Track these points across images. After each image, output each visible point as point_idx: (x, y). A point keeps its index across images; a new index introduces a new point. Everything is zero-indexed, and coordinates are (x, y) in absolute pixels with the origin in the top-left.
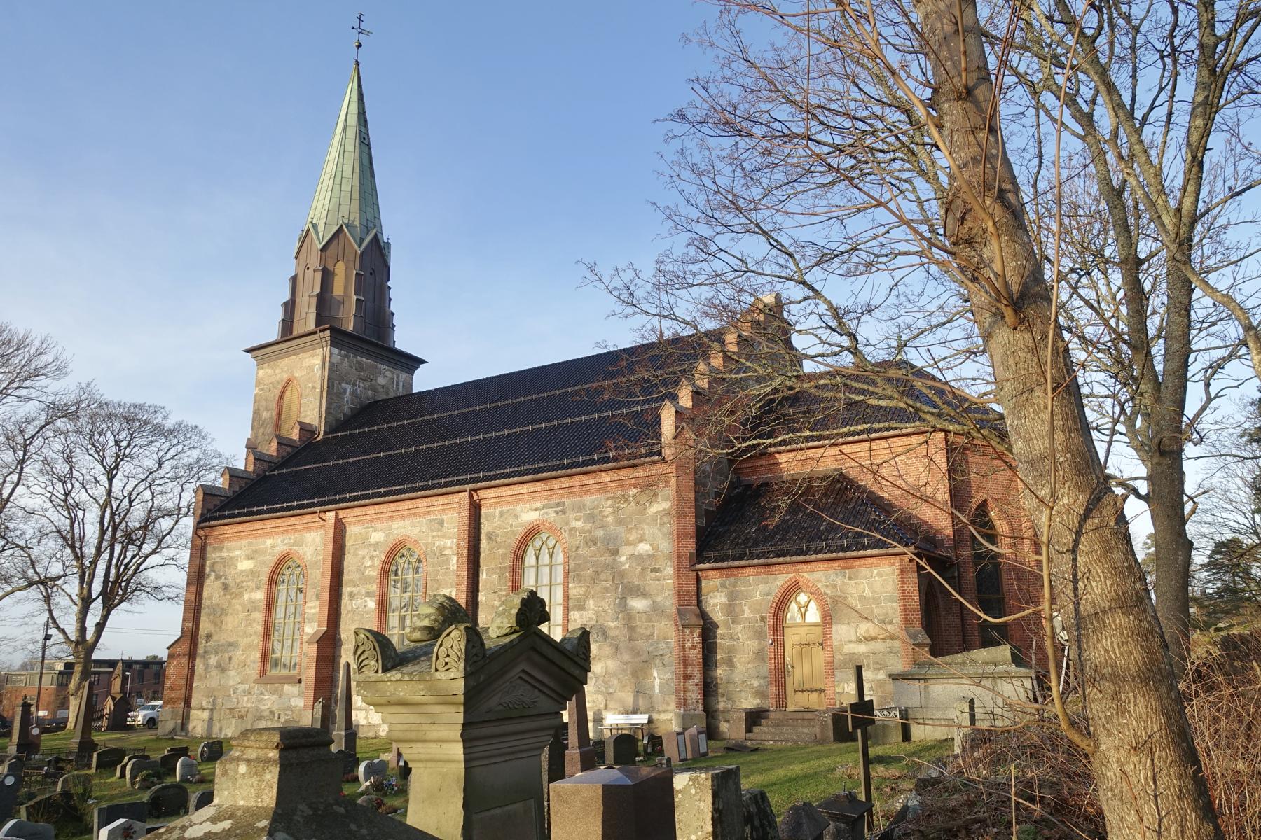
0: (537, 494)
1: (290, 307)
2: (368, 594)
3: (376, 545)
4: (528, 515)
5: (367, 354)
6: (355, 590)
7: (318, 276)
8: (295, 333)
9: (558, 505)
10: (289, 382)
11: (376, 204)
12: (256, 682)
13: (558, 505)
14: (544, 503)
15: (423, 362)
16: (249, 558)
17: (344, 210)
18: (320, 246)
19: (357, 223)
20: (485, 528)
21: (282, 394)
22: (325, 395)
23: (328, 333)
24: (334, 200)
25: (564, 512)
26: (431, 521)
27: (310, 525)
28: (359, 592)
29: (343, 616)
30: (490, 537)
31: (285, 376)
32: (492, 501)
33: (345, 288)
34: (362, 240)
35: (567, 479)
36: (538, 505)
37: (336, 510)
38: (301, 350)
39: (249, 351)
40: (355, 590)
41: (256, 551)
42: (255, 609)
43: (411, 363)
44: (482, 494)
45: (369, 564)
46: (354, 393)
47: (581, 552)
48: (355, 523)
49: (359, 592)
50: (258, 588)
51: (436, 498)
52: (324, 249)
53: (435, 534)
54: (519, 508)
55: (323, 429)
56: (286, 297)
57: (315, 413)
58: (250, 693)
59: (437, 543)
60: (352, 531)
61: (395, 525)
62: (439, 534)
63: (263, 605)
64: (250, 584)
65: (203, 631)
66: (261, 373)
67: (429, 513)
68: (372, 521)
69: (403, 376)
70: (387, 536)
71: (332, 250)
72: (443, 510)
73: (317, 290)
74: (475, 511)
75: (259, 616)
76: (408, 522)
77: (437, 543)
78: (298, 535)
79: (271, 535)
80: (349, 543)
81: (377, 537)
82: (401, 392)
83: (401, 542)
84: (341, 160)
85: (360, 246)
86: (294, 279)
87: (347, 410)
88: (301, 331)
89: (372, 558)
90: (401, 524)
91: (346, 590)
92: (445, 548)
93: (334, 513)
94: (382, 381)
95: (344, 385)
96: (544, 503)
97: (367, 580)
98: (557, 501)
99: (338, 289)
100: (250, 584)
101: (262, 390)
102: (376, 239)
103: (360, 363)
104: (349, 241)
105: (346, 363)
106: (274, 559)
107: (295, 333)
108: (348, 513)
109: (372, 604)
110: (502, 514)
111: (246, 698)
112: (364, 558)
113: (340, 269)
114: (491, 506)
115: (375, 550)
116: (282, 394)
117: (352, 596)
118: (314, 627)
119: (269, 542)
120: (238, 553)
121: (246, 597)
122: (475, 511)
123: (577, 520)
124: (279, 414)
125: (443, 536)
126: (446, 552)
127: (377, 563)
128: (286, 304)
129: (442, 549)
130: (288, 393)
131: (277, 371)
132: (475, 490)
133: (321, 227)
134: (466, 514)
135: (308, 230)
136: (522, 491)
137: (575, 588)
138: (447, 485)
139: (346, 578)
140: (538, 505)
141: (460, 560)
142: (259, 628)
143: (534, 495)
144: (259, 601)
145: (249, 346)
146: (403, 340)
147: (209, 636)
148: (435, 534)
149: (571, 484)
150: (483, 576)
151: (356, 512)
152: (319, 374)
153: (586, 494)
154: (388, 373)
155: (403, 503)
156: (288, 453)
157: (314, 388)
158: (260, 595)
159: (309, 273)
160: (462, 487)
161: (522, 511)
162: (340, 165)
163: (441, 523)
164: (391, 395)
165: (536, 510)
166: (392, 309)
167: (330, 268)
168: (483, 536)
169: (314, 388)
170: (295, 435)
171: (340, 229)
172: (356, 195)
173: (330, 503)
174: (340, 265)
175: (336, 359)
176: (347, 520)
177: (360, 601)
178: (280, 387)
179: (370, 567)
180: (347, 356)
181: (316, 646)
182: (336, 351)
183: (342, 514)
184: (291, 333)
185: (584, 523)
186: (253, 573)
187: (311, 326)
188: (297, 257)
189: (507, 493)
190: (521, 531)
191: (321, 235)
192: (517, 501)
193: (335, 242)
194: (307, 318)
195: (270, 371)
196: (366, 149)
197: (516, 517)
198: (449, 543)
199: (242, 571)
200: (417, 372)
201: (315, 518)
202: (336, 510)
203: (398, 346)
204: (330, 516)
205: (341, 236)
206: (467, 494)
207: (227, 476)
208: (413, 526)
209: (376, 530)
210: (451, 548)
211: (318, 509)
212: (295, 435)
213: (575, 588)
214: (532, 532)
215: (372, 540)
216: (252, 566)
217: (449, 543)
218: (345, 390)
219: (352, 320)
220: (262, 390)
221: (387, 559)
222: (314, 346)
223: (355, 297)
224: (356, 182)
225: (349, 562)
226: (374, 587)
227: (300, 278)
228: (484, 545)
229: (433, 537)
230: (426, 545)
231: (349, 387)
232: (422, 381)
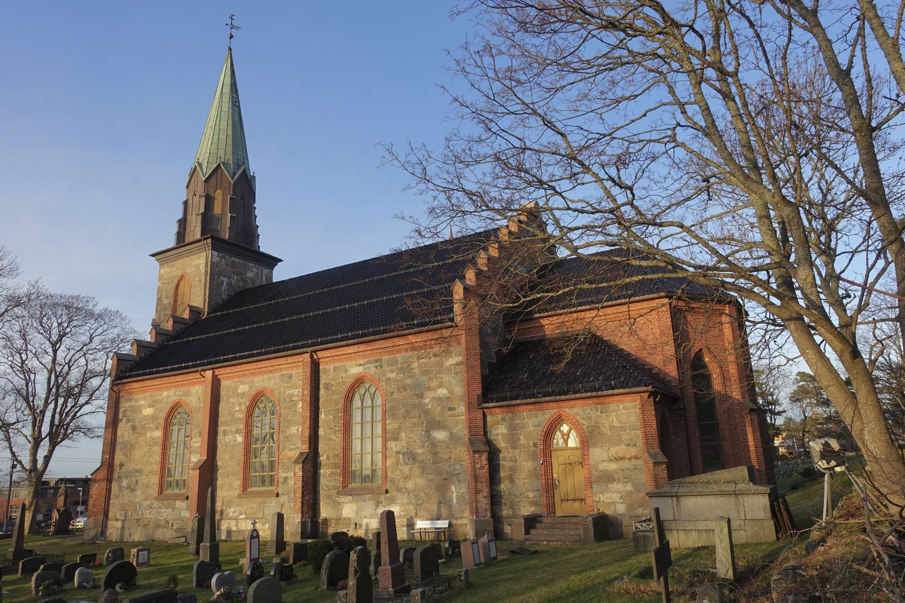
0: (361, 354)
1: (183, 223)
2: (237, 432)
3: (243, 394)
4: (355, 370)
5: (239, 256)
6: (227, 428)
7: (203, 200)
8: (187, 241)
9: (377, 361)
10: (182, 277)
11: (244, 149)
12: (155, 499)
13: (377, 361)
14: (366, 360)
15: (280, 261)
16: (150, 406)
17: (221, 153)
18: (204, 179)
19: (231, 162)
20: (323, 380)
21: (178, 286)
22: (208, 285)
23: (209, 240)
24: (214, 146)
25: (381, 366)
26: (282, 375)
27: (194, 381)
28: (230, 431)
29: (219, 449)
30: (327, 387)
31: (179, 273)
32: (328, 359)
33: (223, 209)
34: (234, 174)
35: (383, 341)
36: (362, 361)
37: (213, 369)
38: (191, 253)
39: (153, 255)
40: (227, 428)
41: (155, 401)
42: (155, 444)
43: (272, 261)
44: (320, 354)
45: (238, 409)
46: (229, 284)
47: (395, 396)
48: (227, 379)
49: (230, 431)
50: (157, 428)
51: (286, 358)
52: (206, 181)
53: (285, 385)
54: (347, 364)
55: (206, 310)
56: (180, 216)
57: (201, 298)
58: (151, 508)
60: (225, 384)
61: (257, 379)
62: (289, 385)
63: (160, 441)
64: (151, 425)
65: (117, 461)
66: (163, 271)
67: (281, 369)
68: (239, 376)
69: (265, 271)
70: (250, 388)
71: (213, 181)
72: (291, 367)
73: (202, 210)
74: (315, 367)
75: (158, 450)
76: (266, 376)
77: (287, 392)
78: (186, 388)
79: (167, 389)
80: (223, 393)
81: (243, 388)
82: (264, 282)
83: (261, 392)
84: (219, 117)
85: (233, 178)
86: (186, 203)
87: (224, 296)
88: (191, 240)
89: (240, 404)
90: (261, 378)
91: (221, 429)
92: (293, 395)
93: (211, 371)
94: (250, 275)
95: (222, 278)
96: (366, 360)
97: (237, 420)
98: (376, 358)
99: (217, 209)
100: (151, 425)
101: (163, 283)
102: (245, 173)
103: (233, 262)
104: (225, 175)
105: (224, 262)
106: (169, 406)
107: (187, 241)
108: (222, 371)
109: (240, 439)
110: (335, 369)
111: (148, 511)
112: (234, 404)
113: (218, 195)
114: (327, 363)
115: (242, 398)
116: (178, 286)
117: (225, 433)
118: (197, 457)
119: (165, 394)
120: (142, 402)
121: (148, 435)
122: (315, 367)
123: (391, 372)
124: (175, 301)
125: (292, 387)
126: (294, 399)
127: (244, 408)
128: (180, 221)
129: (291, 396)
130: (182, 285)
131: (174, 269)
132: (315, 352)
133: (204, 166)
134: (308, 370)
135: (196, 167)
136: (349, 352)
137: (390, 423)
138: (294, 348)
139: (221, 419)
140: (362, 361)
141: (305, 404)
142: (158, 458)
143: (359, 354)
144: (158, 438)
145: (154, 252)
146: (266, 245)
147: (121, 465)
148: (285, 385)
149: (386, 345)
150: (322, 416)
151: (228, 370)
152: (203, 271)
153: (398, 352)
154: (254, 269)
155: (262, 362)
156: (181, 328)
157: (200, 280)
158: (158, 434)
159: (196, 198)
160: (305, 350)
161: (350, 367)
162: (218, 121)
163: (290, 377)
164: (257, 284)
165: (361, 365)
166: (257, 223)
167: (212, 194)
168: (321, 386)
169: (200, 280)
170: (186, 315)
171: (218, 166)
172: (230, 142)
173: (209, 364)
174: (219, 192)
175: (216, 259)
176: (222, 376)
177: (231, 437)
178: (176, 281)
179: (238, 411)
180: (224, 257)
181: (198, 471)
182: (215, 253)
183: (217, 372)
184: (184, 242)
185: (397, 374)
186: (153, 417)
187: (198, 236)
188: (187, 187)
189: (338, 353)
190: (350, 381)
191: (205, 171)
192: (346, 359)
193: (215, 176)
194: (195, 230)
195: (169, 270)
196: (236, 109)
197: (346, 371)
198: (296, 392)
199: (145, 416)
200: (276, 268)
201: (198, 375)
202: (213, 369)
203: (261, 250)
204: (209, 374)
205: (219, 171)
206: (308, 355)
207: (135, 346)
208: (269, 379)
209: (243, 384)
210: (298, 395)
211: (200, 369)
212: (186, 315)
213: (390, 423)
214: (359, 382)
216: (152, 412)
218: (223, 282)
219: (228, 231)
220: (163, 283)
221: (251, 405)
222: (200, 250)
223: (229, 215)
224: (230, 133)
225: (223, 407)
226: (242, 426)
227: (190, 201)
228: (322, 392)
229: (285, 388)
230: (280, 393)
231: (225, 280)
232: (280, 274)
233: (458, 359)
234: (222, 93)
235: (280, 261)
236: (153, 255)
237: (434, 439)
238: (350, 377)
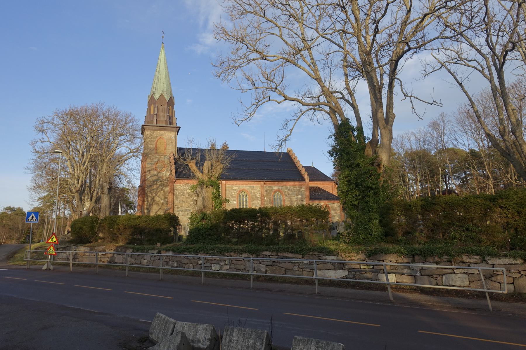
2: (234, 200)
3: (235, 190)
13: (282, 187)
26: (251, 186)
38: (165, 130)
54: (273, 186)
59: (253, 191)
70: (238, 188)
76: (245, 186)
77: (253, 191)
81: (234, 188)
89: (234, 193)
90: (242, 186)
97: (234, 197)
123: (286, 190)
125: (255, 190)
127: (236, 194)
129: (254, 193)
147: (178, 208)
157: (172, 142)
163: (254, 187)
197: (272, 188)
215: (234, 188)
233: (304, 189)
238: (274, 190)
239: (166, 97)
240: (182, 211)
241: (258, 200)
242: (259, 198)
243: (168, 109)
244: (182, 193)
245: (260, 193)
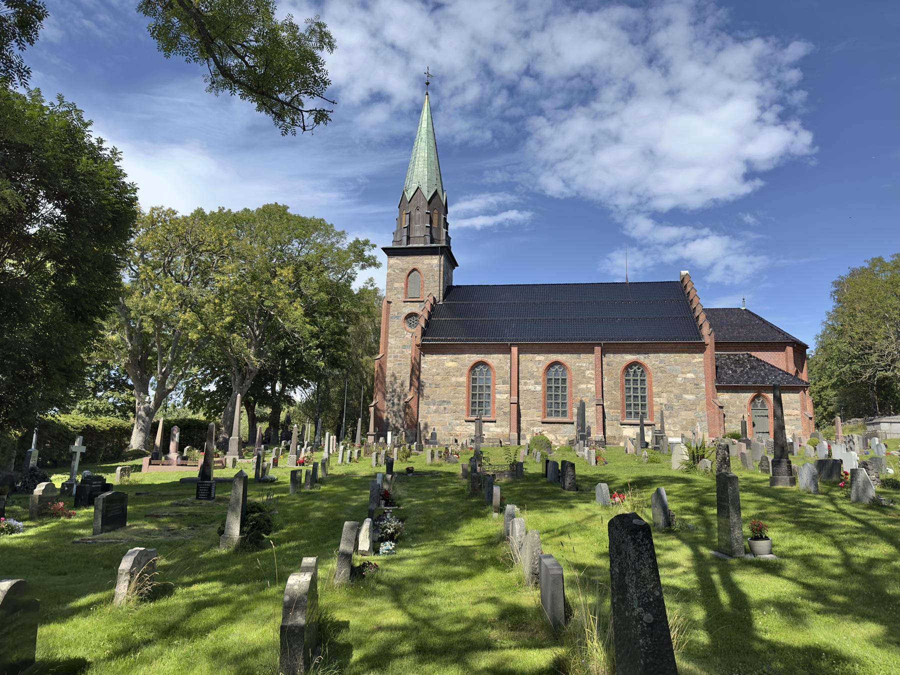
2: (536, 383)
3: (540, 361)
10: (414, 270)
15: (457, 266)
18: (428, 200)
50: (462, 376)
52: (429, 202)
55: (441, 298)
63: (465, 385)
109: (539, 388)
116: (409, 275)
139: (520, 375)
145: (385, 246)
152: (437, 269)
158: (464, 379)
178: (408, 272)
185: (660, 363)
186: (458, 369)
195: (398, 262)
198: (584, 365)
205: (437, 196)
217: (584, 365)
226: (541, 380)
227: (413, 213)
228: (605, 367)
234: (428, 131)
235: (457, 266)
236: (384, 249)
237: (685, 399)
239: (425, 193)
240: (434, 405)
241: (588, 383)
242: (591, 378)
243: (428, 215)
244: (434, 370)
245: (592, 369)
